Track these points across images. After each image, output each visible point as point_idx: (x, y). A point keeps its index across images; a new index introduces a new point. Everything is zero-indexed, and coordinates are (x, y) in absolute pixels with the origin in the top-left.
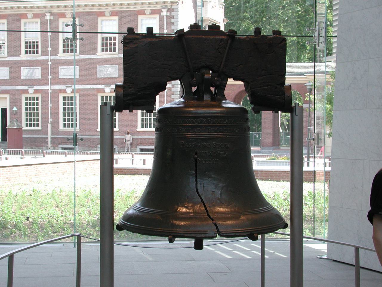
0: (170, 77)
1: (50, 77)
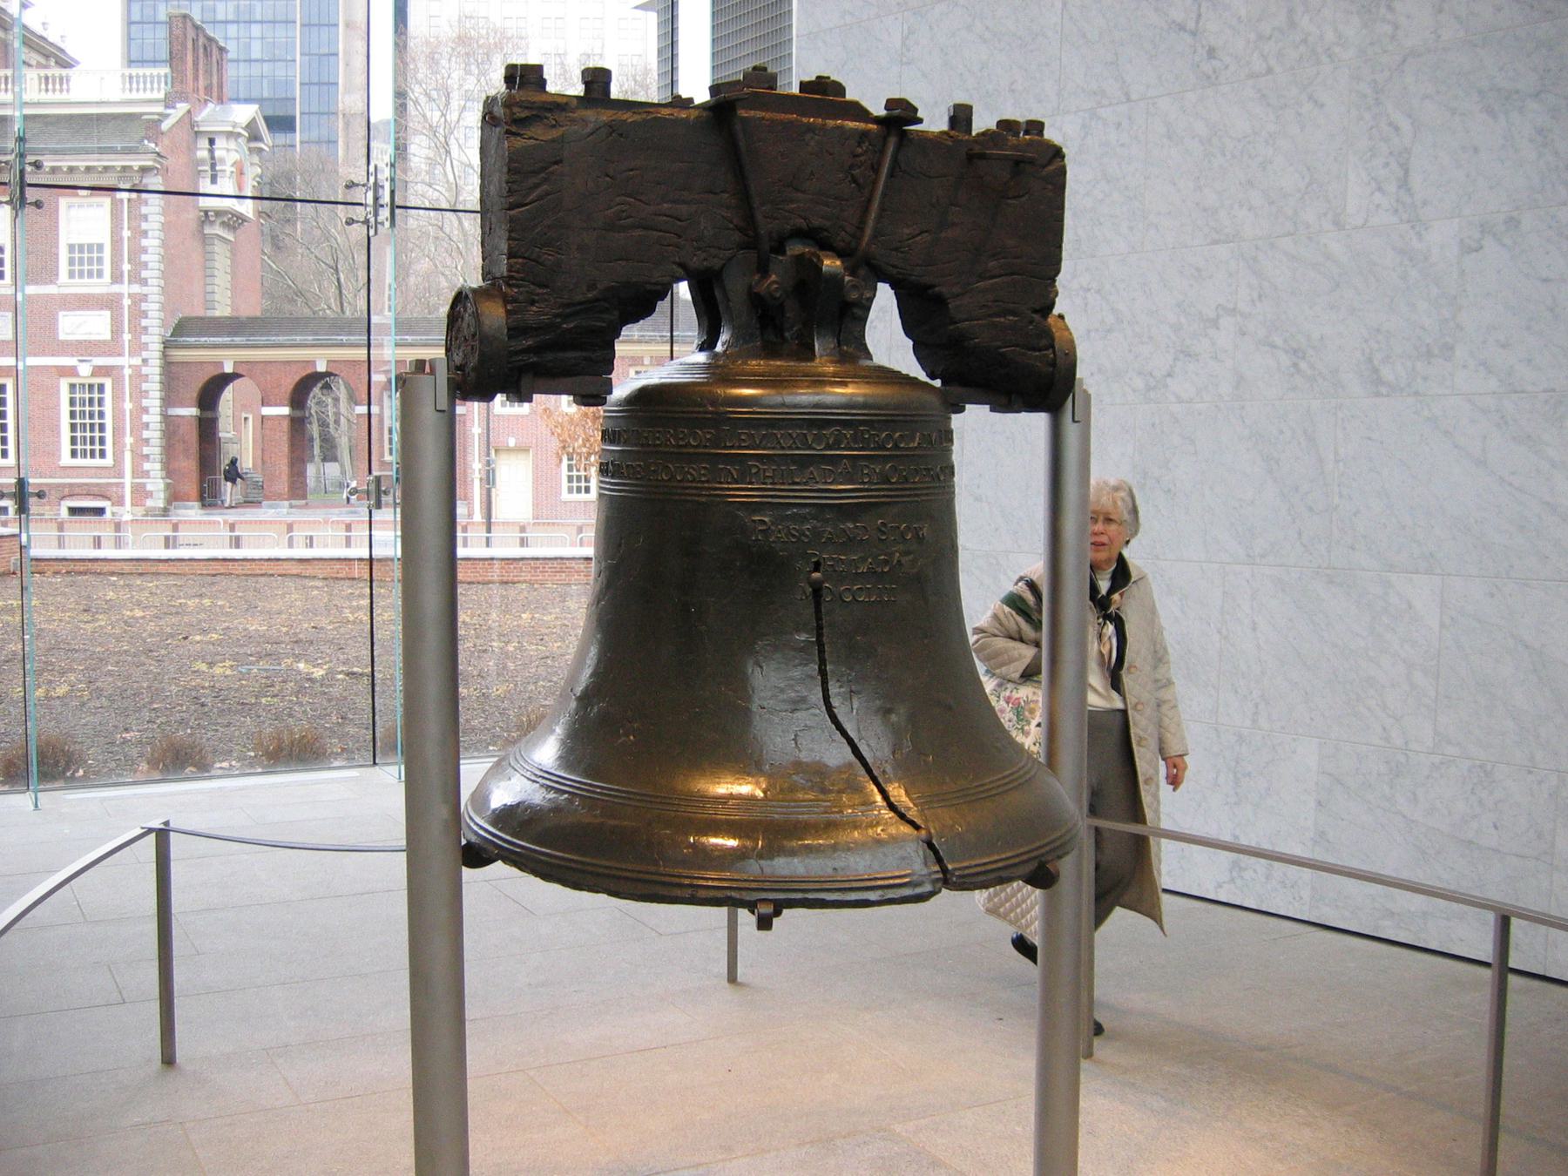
0: (681, 265)
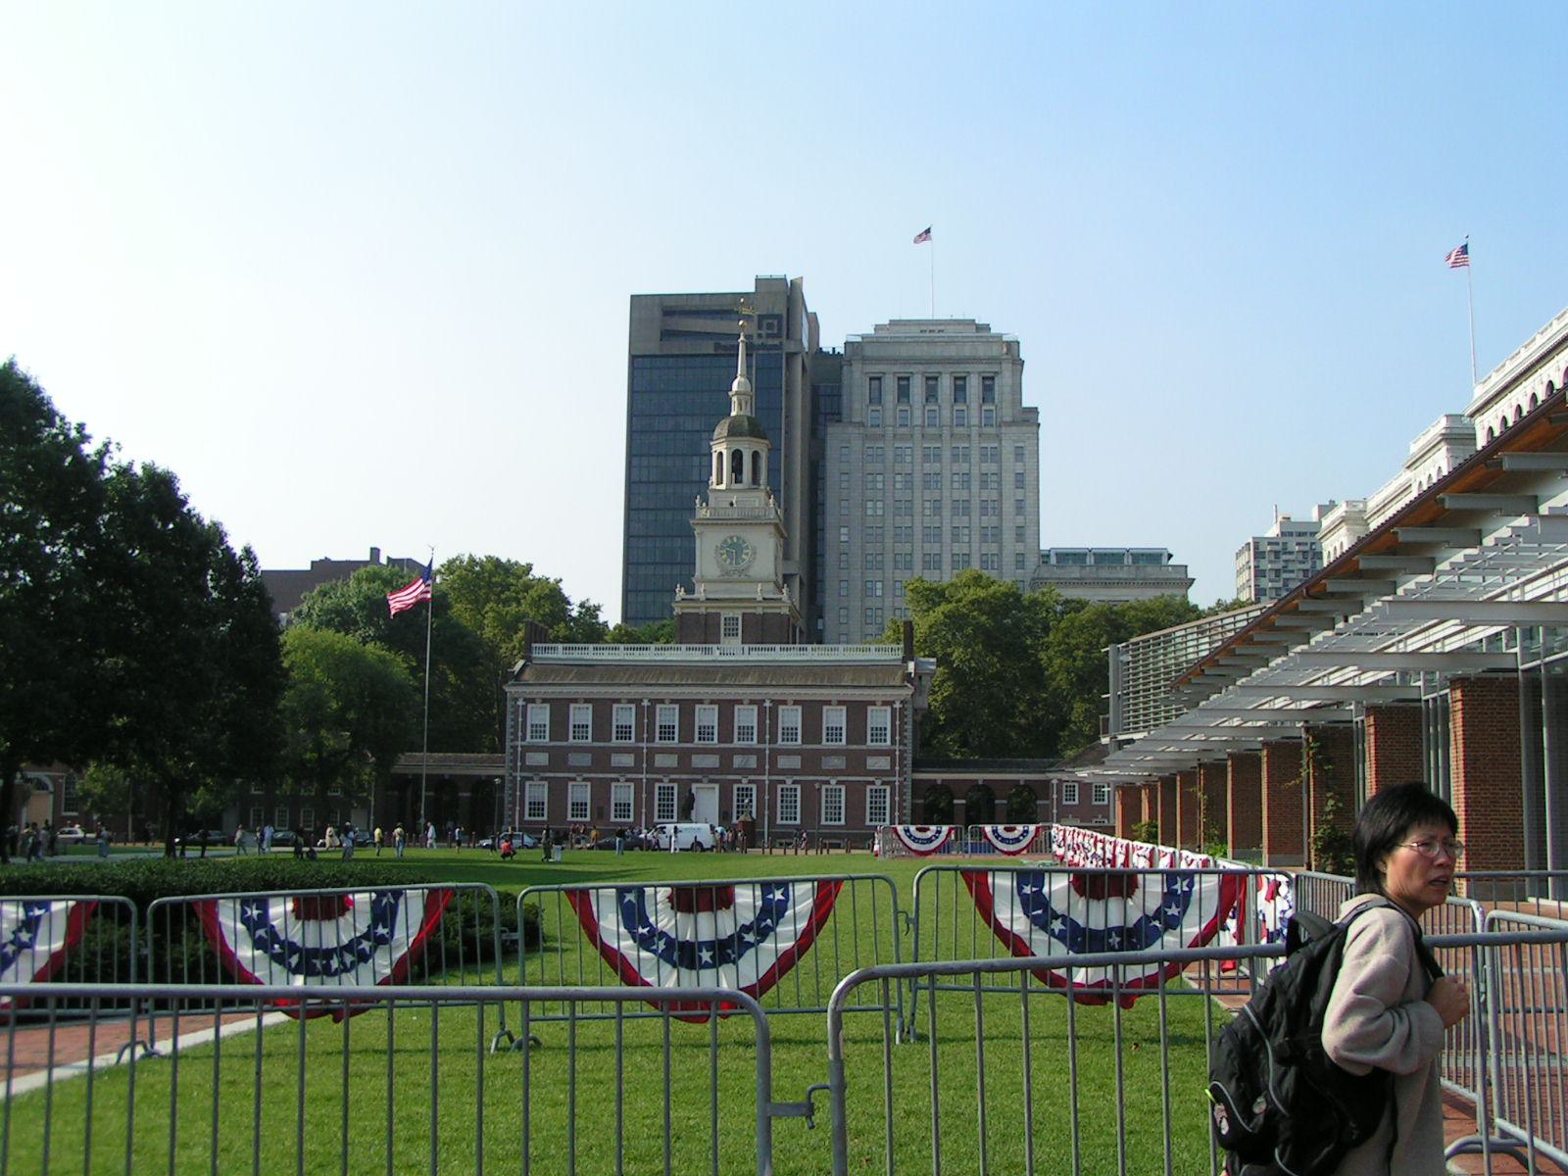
1: (767, 767)
